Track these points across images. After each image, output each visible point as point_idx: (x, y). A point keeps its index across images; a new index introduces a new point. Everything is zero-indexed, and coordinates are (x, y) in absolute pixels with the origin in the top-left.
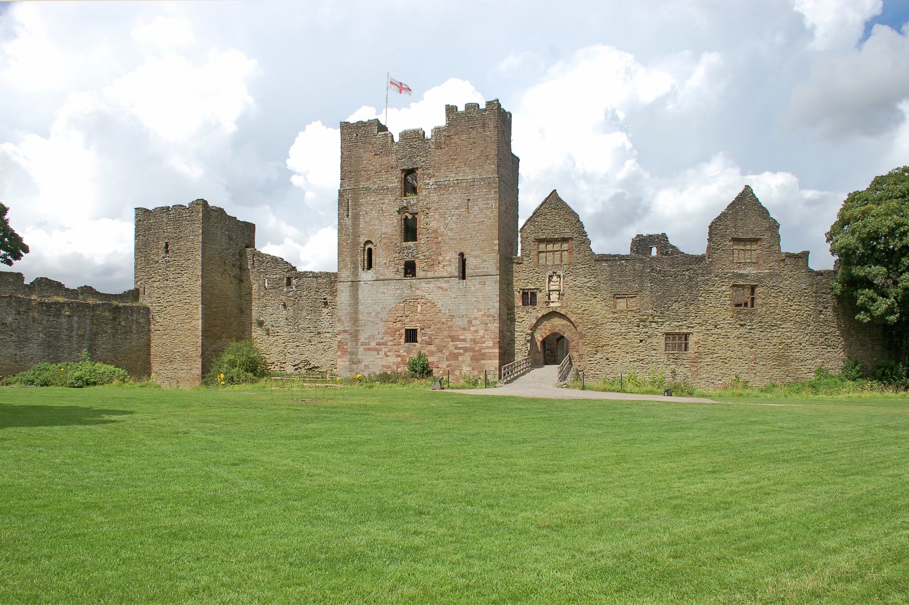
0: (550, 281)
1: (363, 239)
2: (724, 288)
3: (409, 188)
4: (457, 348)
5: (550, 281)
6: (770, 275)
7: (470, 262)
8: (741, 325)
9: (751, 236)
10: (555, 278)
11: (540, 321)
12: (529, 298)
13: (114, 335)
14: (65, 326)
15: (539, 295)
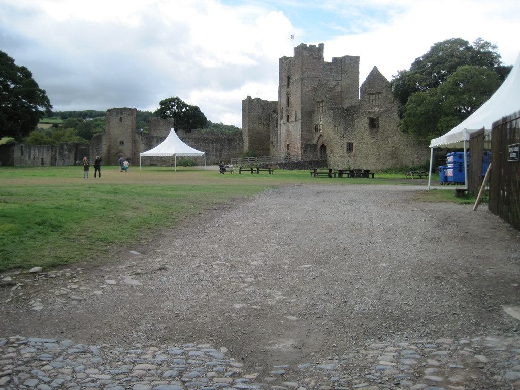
0: (320, 120)
1: (282, 107)
2: (365, 120)
3: (288, 85)
4: (295, 152)
5: (320, 120)
6: (386, 111)
7: (297, 114)
8: (373, 138)
9: (377, 91)
10: (322, 119)
11: (319, 138)
12: (316, 129)
13: (229, 150)
14: (211, 147)
15: (319, 127)
